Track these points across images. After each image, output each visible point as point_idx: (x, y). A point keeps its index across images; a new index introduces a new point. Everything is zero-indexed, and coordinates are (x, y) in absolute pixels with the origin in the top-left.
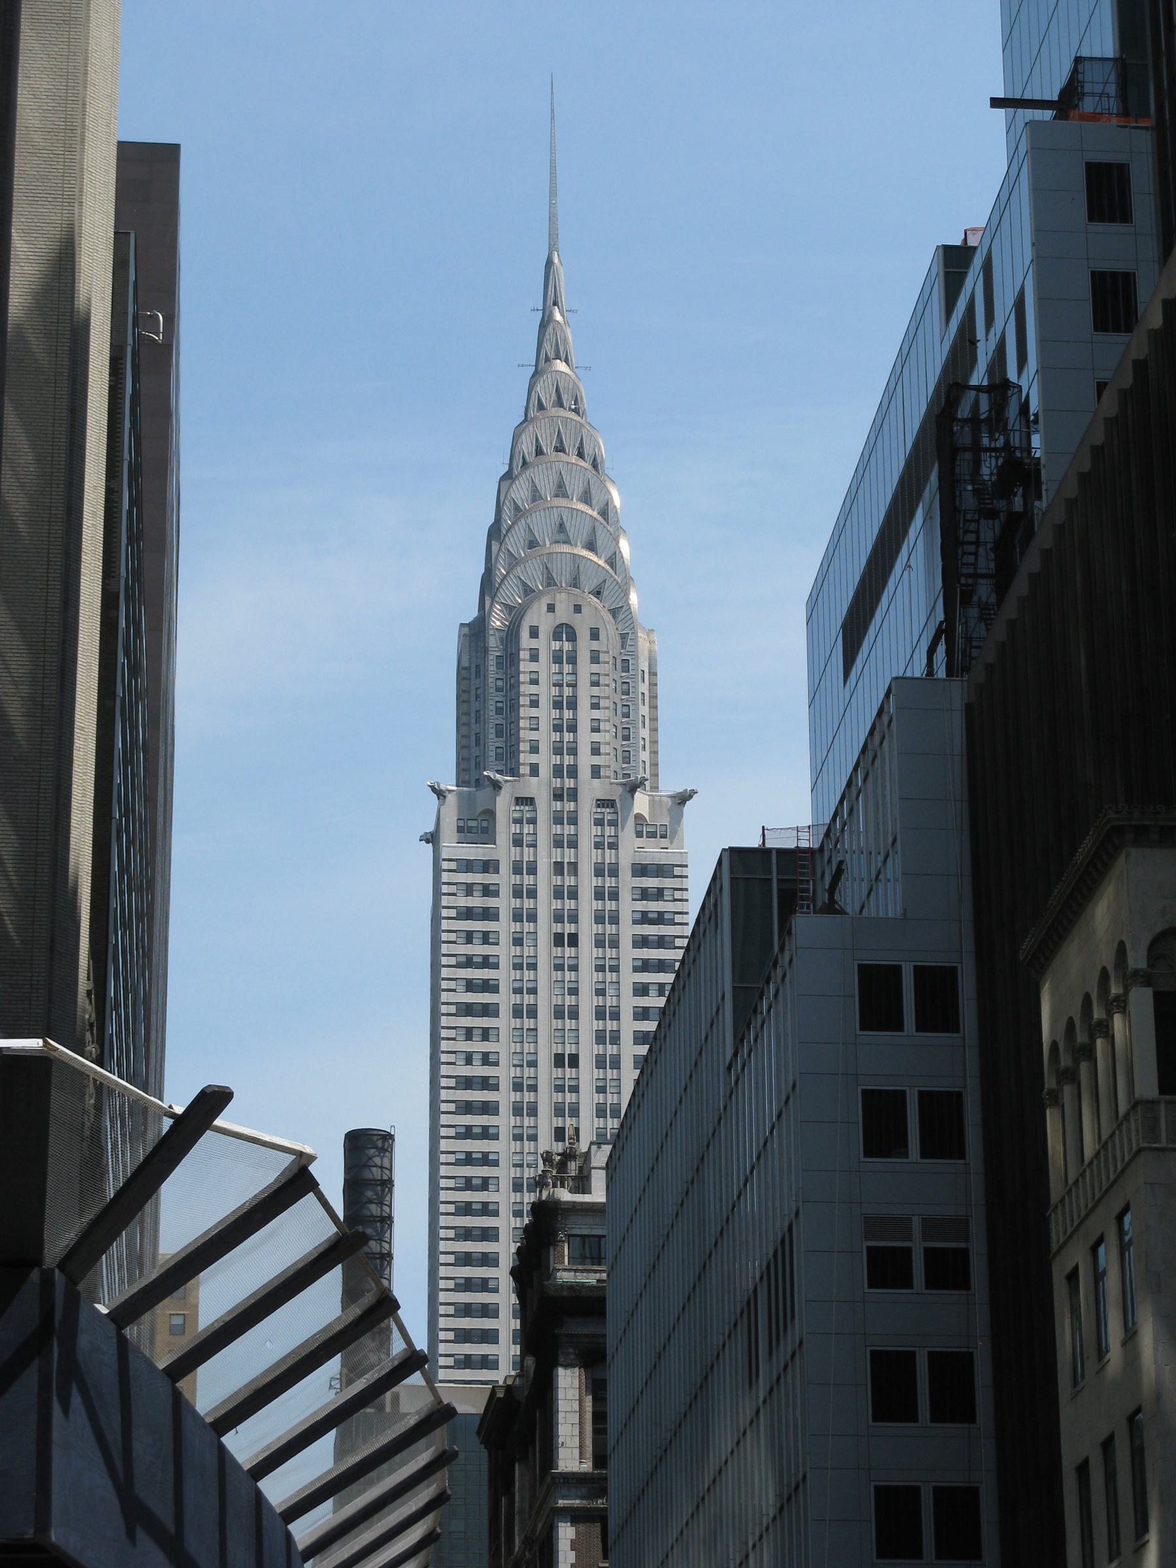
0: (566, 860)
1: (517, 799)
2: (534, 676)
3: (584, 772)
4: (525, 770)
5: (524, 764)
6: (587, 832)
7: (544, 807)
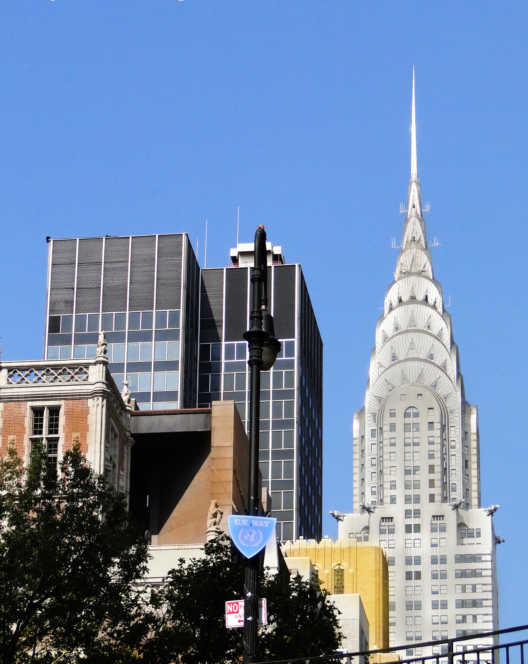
1: (383, 518)
2: (393, 441)
4: (387, 500)
5: (387, 496)
7: (400, 522)
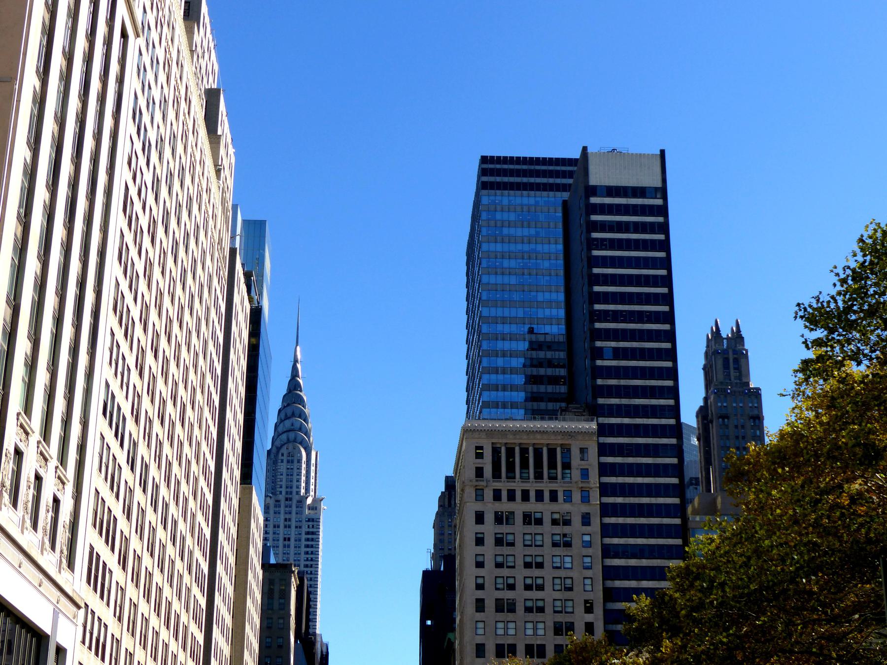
6: (294, 509)
7: (283, 503)
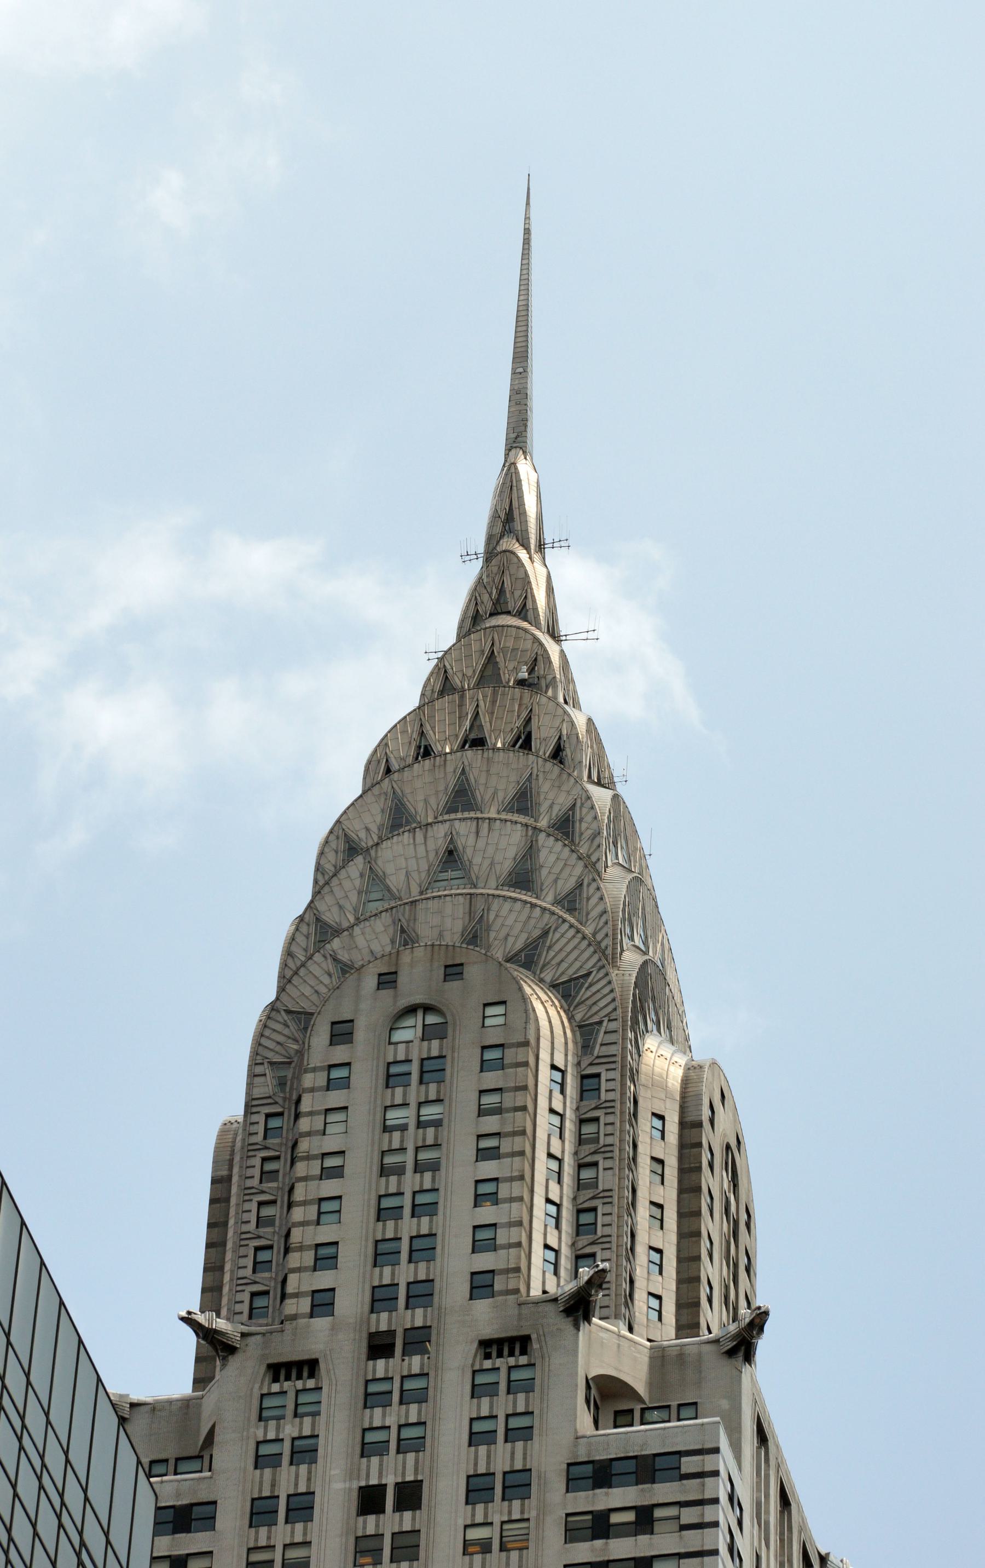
0: (390, 1480)
3: (452, 1288)
6: (453, 1408)
